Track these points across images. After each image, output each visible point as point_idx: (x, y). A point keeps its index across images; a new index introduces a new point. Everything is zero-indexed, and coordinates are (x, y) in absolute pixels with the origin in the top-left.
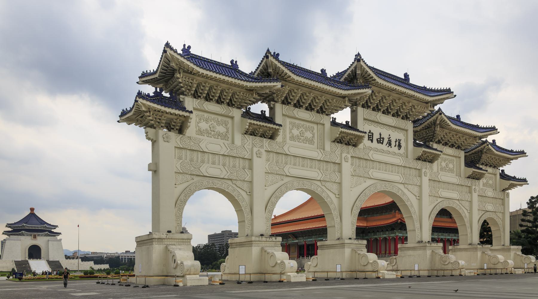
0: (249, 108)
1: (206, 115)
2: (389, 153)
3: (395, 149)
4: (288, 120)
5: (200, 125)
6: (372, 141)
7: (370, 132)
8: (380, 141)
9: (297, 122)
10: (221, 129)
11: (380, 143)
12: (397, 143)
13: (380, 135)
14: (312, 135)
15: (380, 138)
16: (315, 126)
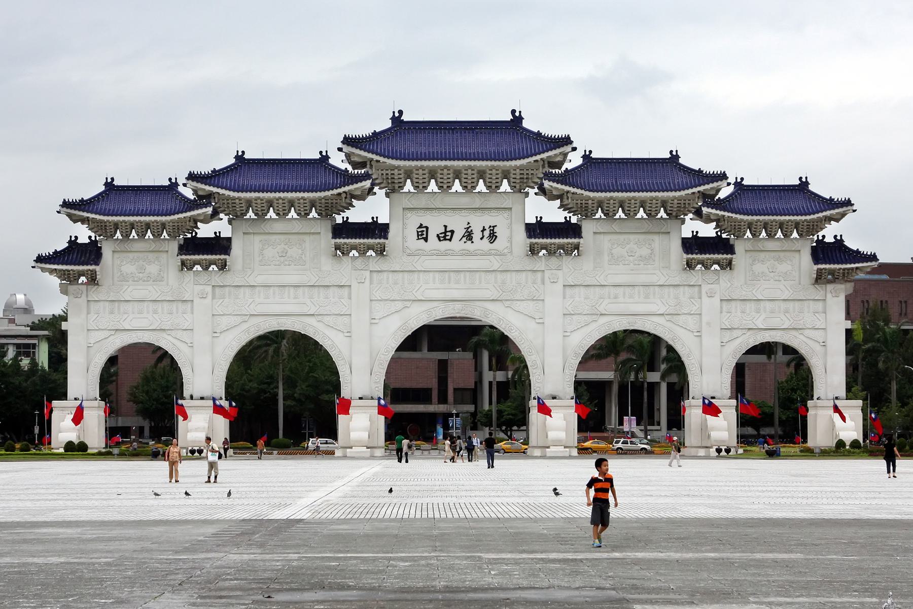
0: (196, 233)
1: (131, 255)
2: (469, 254)
3: (480, 244)
4: (257, 238)
5: (123, 268)
6: (426, 239)
7: (421, 226)
8: (446, 235)
10: (153, 269)
11: (445, 239)
12: (487, 233)
13: (446, 227)
14: (300, 251)
15: (446, 231)
16: (307, 238)
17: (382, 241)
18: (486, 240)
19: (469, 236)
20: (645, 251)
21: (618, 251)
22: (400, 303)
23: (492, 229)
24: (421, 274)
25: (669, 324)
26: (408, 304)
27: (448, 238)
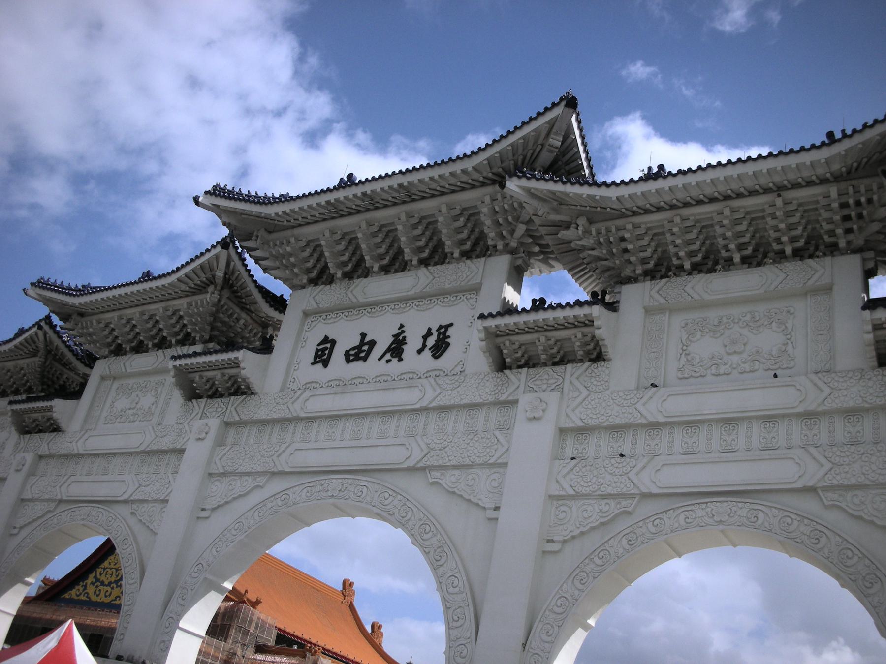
6: (326, 364)
7: (326, 340)
8: (361, 351)
9: (131, 381)
11: (357, 358)
12: (431, 341)
13: (363, 336)
14: (153, 400)
15: (362, 343)
17: (232, 355)
18: (427, 353)
19: (396, 349)
20: (768, 340)
21: (706, 347)
22: (250, 479)
23: (443, 332)
24: (301, 426)
25: (833, 517)
26: (261, 480)
27: (363, 355)
